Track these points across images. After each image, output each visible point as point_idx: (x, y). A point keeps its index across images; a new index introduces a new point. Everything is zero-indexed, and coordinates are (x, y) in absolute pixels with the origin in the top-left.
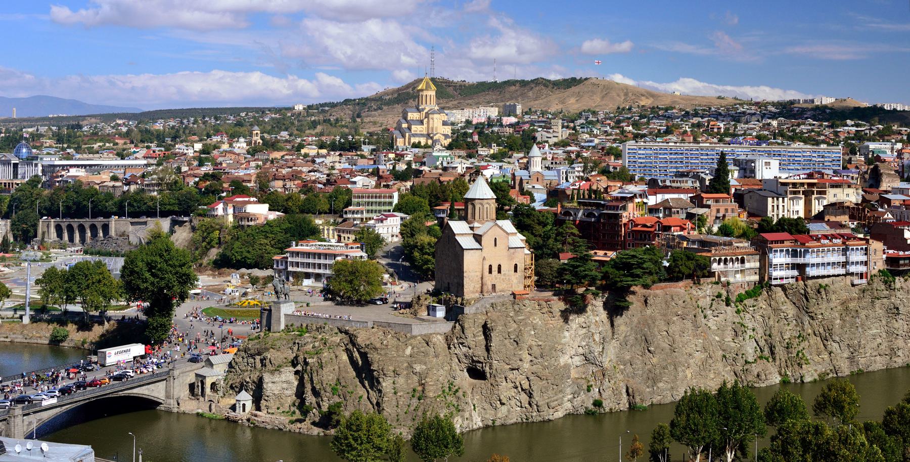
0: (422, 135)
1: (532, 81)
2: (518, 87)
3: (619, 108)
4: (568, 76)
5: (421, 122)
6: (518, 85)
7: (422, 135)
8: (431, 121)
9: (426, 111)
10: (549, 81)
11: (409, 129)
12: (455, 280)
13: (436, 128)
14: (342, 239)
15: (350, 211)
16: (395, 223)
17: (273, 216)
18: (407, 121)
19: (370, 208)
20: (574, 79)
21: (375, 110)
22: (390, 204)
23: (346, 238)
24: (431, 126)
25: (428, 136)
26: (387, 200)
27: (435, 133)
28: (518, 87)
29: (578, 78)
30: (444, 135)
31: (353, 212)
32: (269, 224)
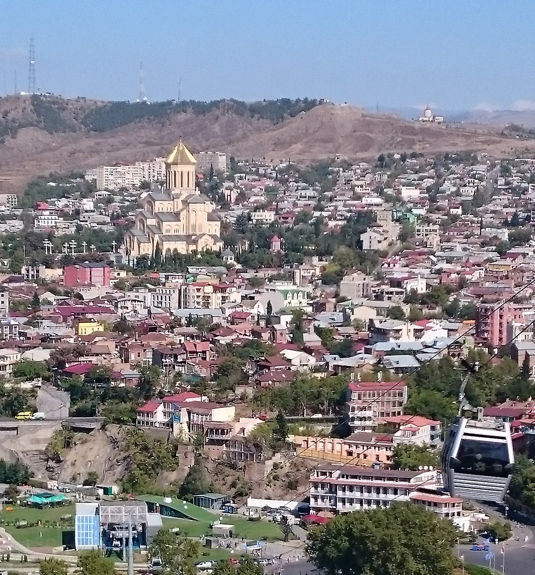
0: (178, 238)
2: (190, 114)
5: (176, 216)
6: (190, 110)
7: (178, 238)
8: (192, 214)
9: (183, 198)
10: (242, 104)
11: (159, 228)
13: (201, 226)
18: (156, 216)
20: (286, 102)
24: (192, 222)
25: (189, 239)
26: (397, 399)
27: (198, 233)
28: (190, 114)
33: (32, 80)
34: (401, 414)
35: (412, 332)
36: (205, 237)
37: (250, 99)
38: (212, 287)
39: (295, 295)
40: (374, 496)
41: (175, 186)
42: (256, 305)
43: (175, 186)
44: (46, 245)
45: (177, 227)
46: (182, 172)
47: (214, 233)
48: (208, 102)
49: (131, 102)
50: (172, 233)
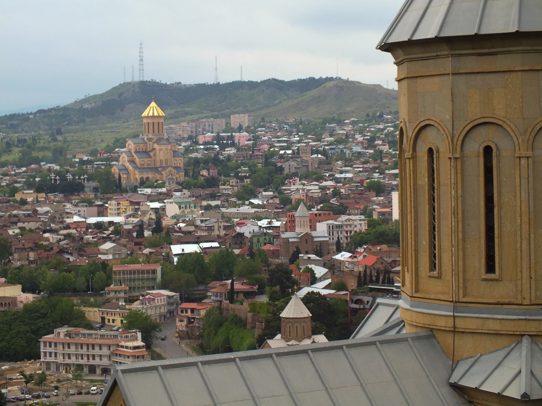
1: (264, 82)
3: (368, 115)
4: (305, 76)
14: (106, 321)
15: (112, 291)
16: (163, 303)
17: (30, 297)
19: (133, 284)
20: (312, 79)
21: (77, 123)
22: (154, 279)
23: (111, 321)
29: (317, 77)
30: (176, 168)
31: (116, 292)
32: (28, 309)
33: (141, 71)
34: (155, 288)
35: (222, 227)
36: (170, 168)
37: (287, 78)
38: (128, 202)
39: (188, 206)
40: (84, 351)
41: (149, 133)
42: (149, 213)
43: (149, 133)
44: (53, 178)
45: (150, 162)
46: (153, 123)
47: (179, 165)
48: (259, 81)
49: (209, 84)
50: (146, 166)
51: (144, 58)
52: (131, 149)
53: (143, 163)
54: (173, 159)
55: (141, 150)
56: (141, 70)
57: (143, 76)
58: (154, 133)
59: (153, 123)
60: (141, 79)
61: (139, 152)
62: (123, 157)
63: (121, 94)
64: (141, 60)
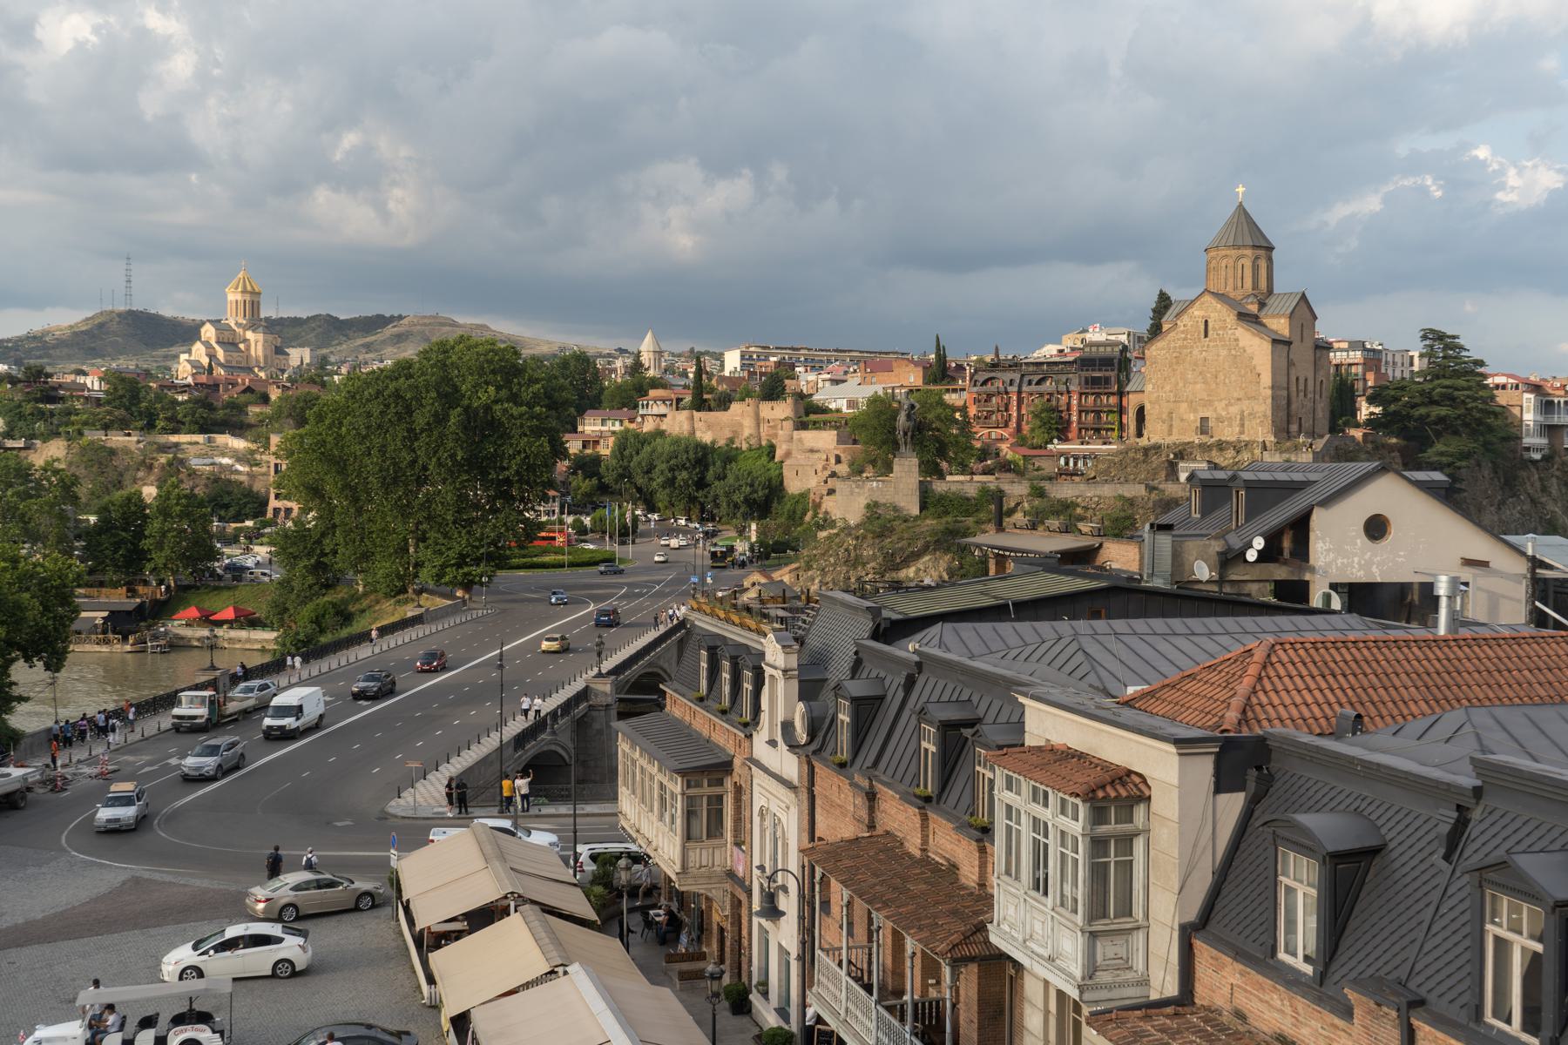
12: (1234, 410)
29: (387, 315)
50: (234, 364)
51: (132, 279)
52: (210, 338)
53: (229, 358)
54: (274, 356)
55: (226, 341)
56: (128, 295)
57: (131, 304)
58: (245, 316)
59: (245, 301)
60: (128, 308)
61: (224, 343)
62: (198, 349)
63: (101, 326)
64: (129, 281)
